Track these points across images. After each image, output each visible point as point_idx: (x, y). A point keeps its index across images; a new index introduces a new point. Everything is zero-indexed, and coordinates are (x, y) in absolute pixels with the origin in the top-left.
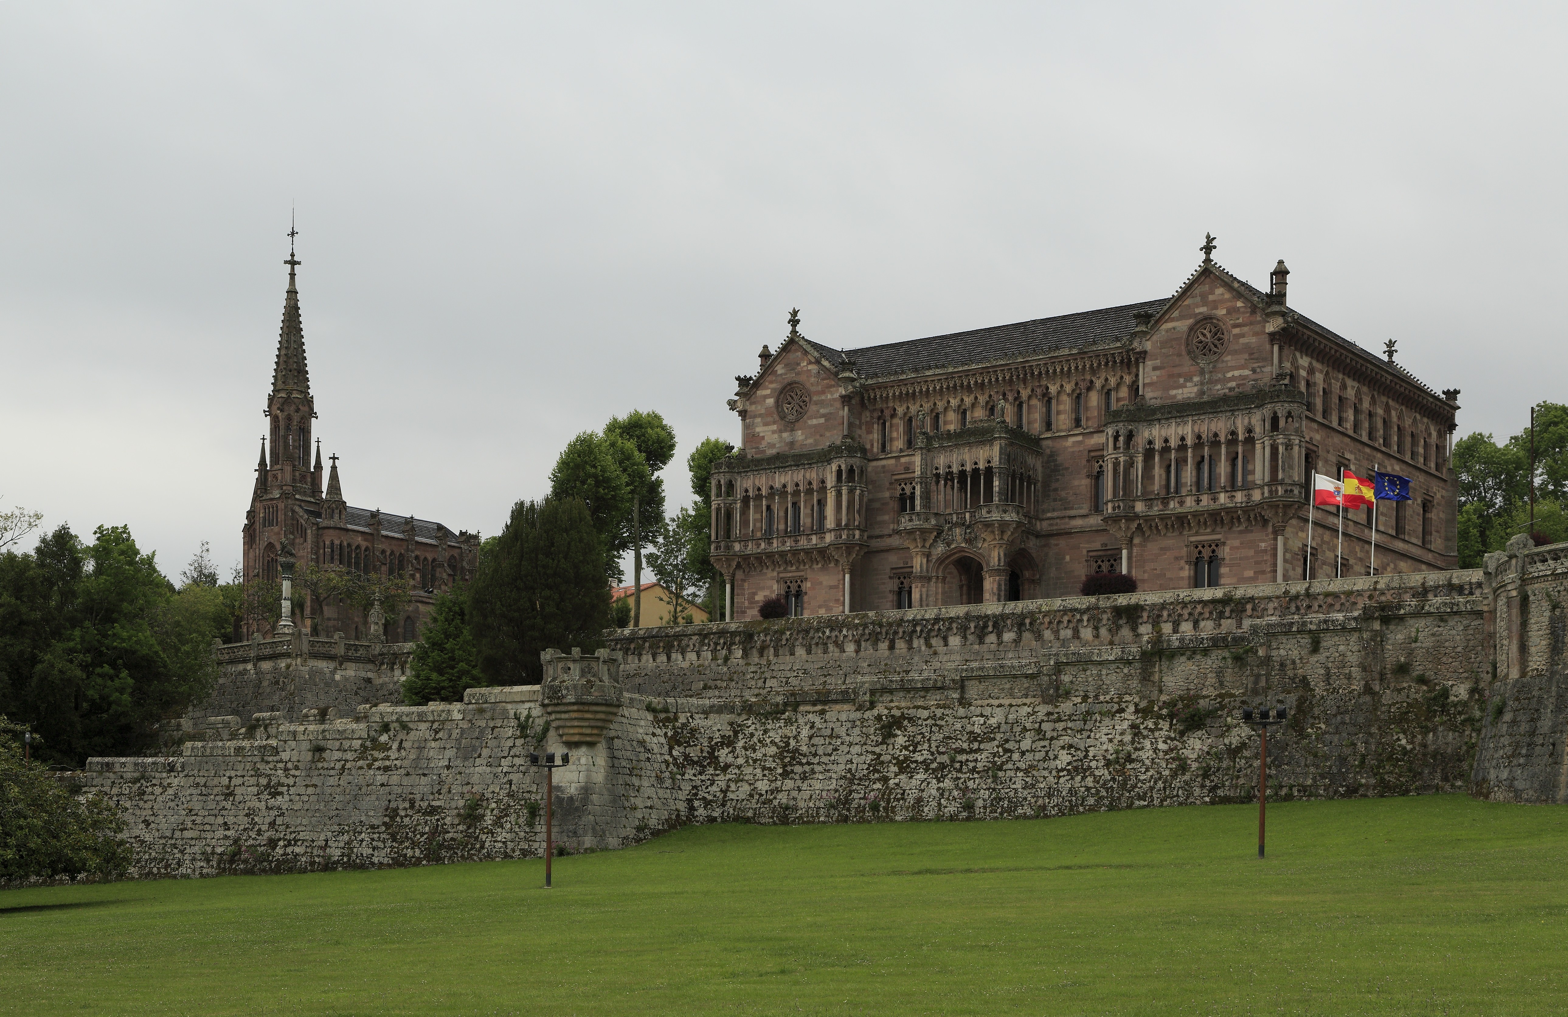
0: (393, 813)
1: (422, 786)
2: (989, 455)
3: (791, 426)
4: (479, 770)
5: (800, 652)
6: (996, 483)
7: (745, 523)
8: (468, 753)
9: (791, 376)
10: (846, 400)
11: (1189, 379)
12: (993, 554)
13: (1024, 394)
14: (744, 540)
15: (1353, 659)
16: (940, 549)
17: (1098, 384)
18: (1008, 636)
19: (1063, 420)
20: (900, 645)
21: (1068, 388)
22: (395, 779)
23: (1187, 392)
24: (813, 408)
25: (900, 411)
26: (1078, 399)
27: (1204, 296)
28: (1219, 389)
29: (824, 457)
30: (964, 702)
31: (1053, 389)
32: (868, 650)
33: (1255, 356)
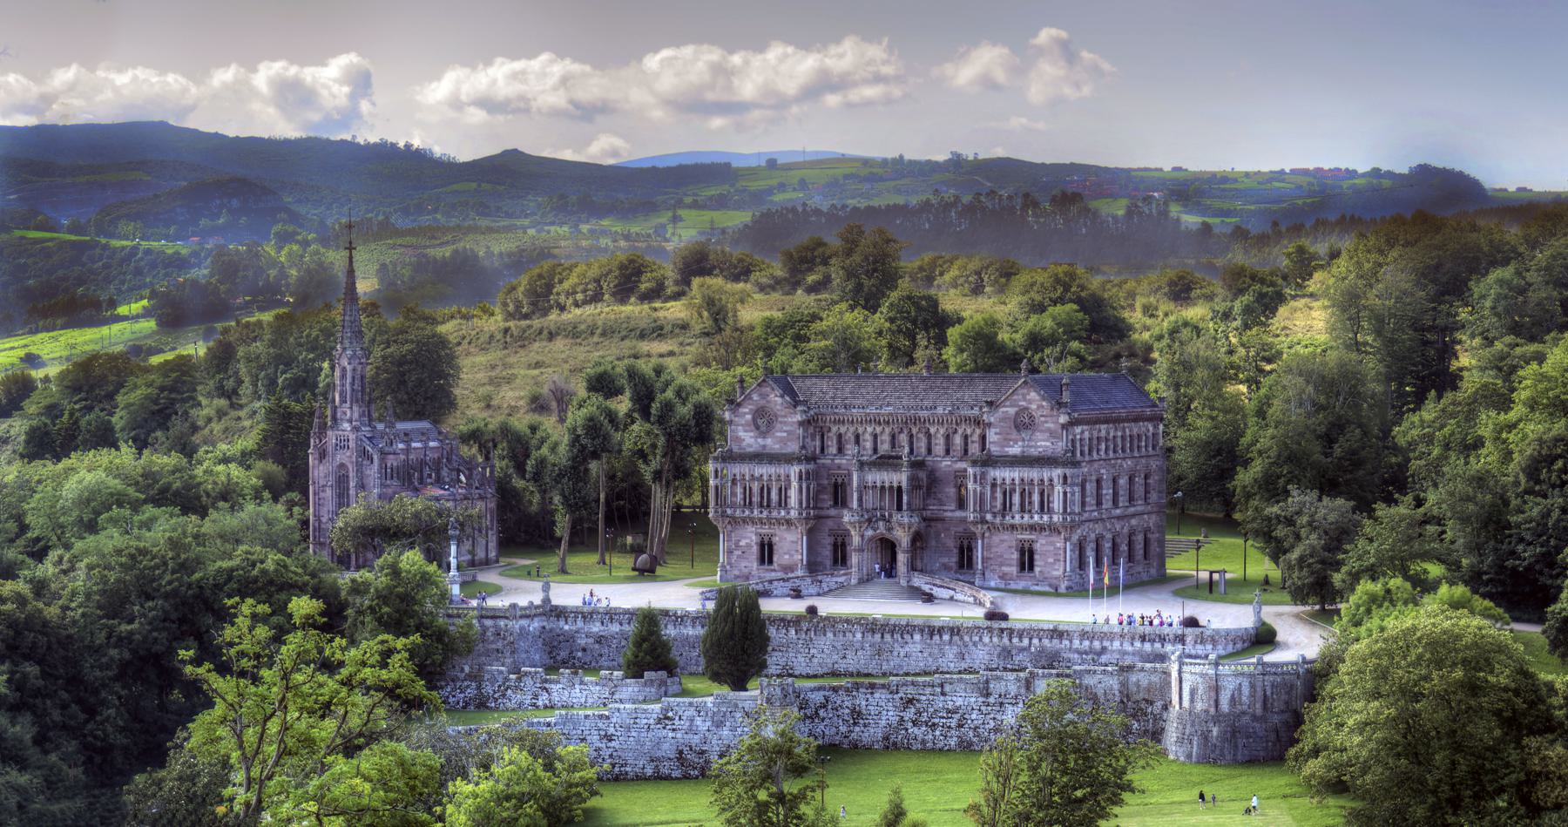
0: (681, 752)
1: (695, 740)
2: (901, 478)
3: (764, 435)
4: (725, 732)
5: (830, 635)
6: (905, 497)
7: (734, 494)
8: (719, 725)
9: (763, 402)
10: (801, 424)
11: (1016, 442)
12: (903, 537)
13: (914, 431)
14: (733, 506)
15: (1116, 687)
16: (870, 533)
17: (960, 431)
18: (946, 637)
19: (939, 448)
20: (888, 637)
21: (942, 431)
22: (679, 735)
23: (1015, 450)
24: (778, 426)
25: (834, 429)
26: (948, 438)
27: (1024, 396)
28: (1034, 452)
29: (788, 459)
30: (943, 694)
31: (932, 430)
32: (869, 637)
33: (1052, 434)
